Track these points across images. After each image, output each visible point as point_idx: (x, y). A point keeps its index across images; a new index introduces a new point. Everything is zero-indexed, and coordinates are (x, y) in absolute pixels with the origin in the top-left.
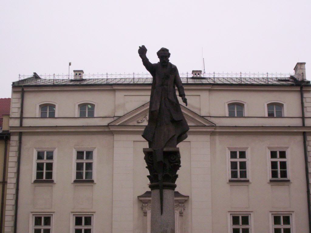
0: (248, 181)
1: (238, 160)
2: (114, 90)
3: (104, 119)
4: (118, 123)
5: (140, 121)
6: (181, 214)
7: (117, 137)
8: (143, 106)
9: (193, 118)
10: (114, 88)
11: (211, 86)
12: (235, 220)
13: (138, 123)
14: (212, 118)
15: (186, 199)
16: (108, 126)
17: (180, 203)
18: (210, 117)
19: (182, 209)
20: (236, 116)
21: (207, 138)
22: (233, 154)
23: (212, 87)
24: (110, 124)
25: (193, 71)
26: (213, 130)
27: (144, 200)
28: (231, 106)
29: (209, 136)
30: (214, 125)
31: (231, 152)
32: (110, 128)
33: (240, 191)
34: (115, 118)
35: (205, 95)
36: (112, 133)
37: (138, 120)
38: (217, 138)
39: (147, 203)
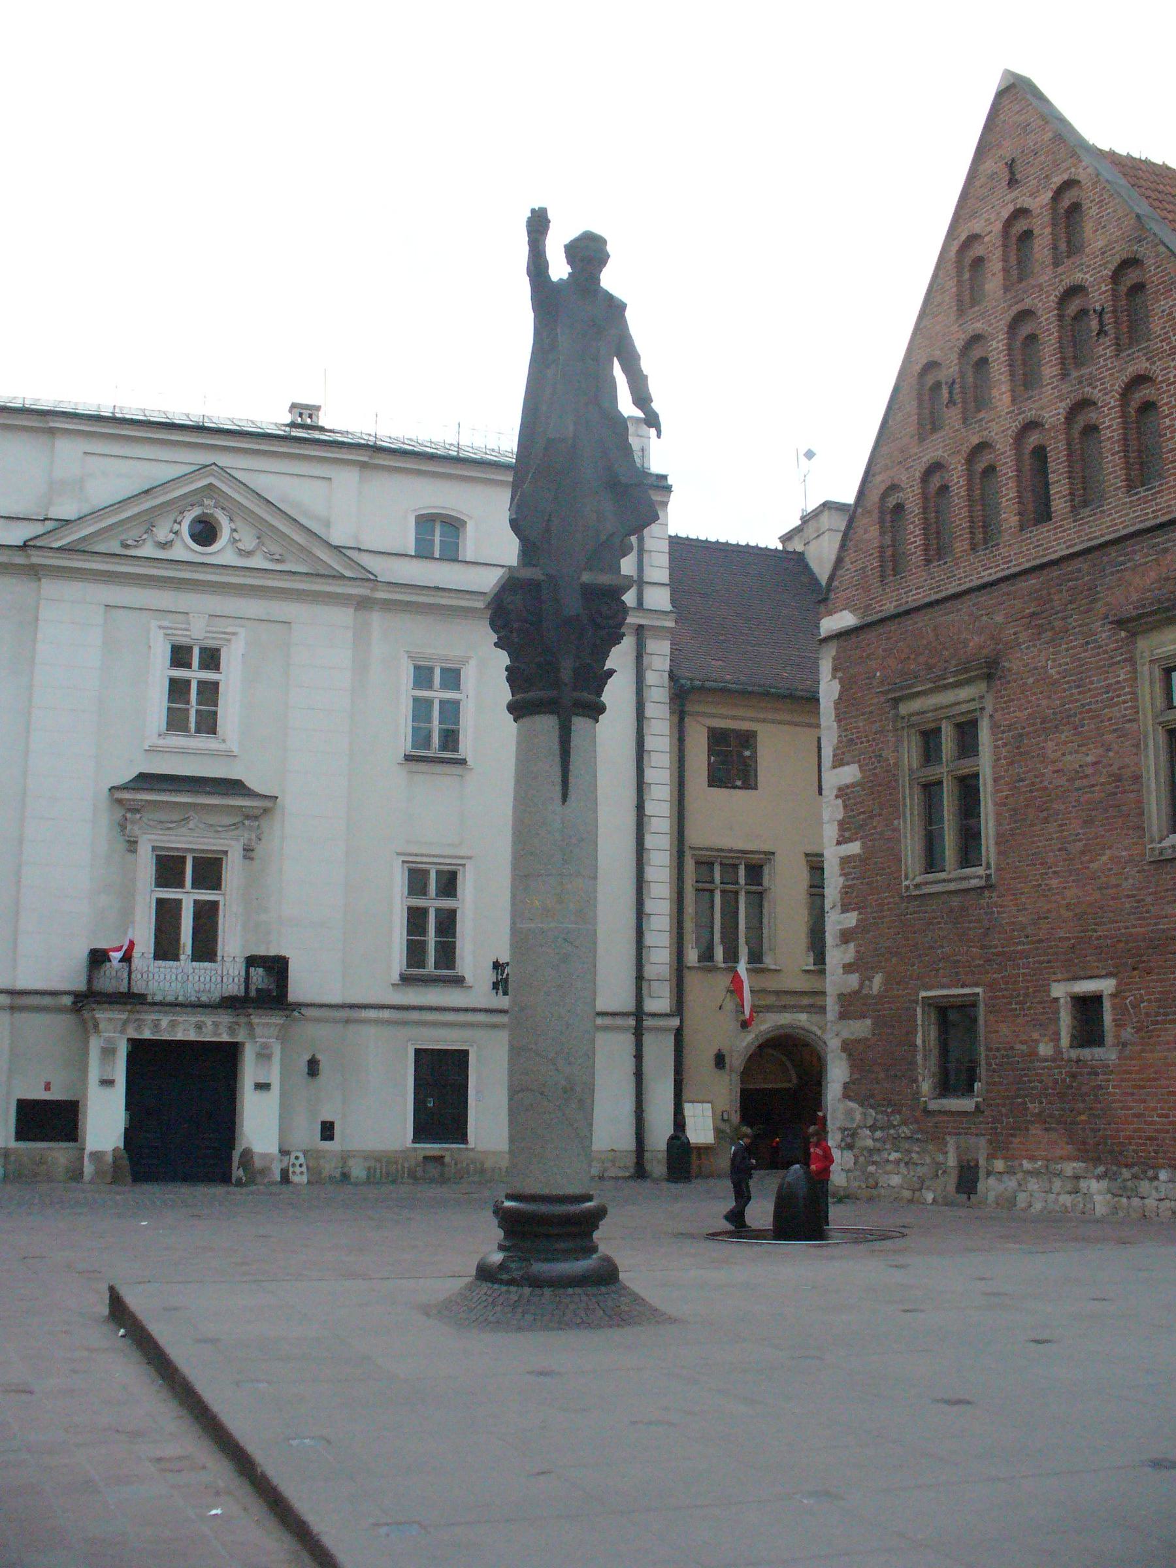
0: (463, 762)
1: (438, 695)
2: (52, 431)
3: (13, 524)
4: (57, 540)
5: (129, 542)
6: (248, 852)
7: (50, 587)
8: (147, 492)
9: (303, 549)
10: (52, 425)
11: (369, 453)
12: (417, 880)
13: (126, 546)
14: (364, 555)
15: (267, 804)
16: (25, 546)
17: (248, 817)
18: (359, 549)
19: (254, 837)
20: (437, 555)
21: (344, 616)
22: (423, 676)
23: (370, 457)
24: (30, 543)
25: (294, 406)
26: (367, 592)
27: (129, 800)
28: (425, 522)
29: (352, 610)
30: (372, 577)
31: (417, 668)
32: (29, 557)
33: (435, 792)
34: (50, 525)
35: (346, 479)
36: (34, 572)
37: (124, 537)
38: (376, 619)
39: (138, 811)
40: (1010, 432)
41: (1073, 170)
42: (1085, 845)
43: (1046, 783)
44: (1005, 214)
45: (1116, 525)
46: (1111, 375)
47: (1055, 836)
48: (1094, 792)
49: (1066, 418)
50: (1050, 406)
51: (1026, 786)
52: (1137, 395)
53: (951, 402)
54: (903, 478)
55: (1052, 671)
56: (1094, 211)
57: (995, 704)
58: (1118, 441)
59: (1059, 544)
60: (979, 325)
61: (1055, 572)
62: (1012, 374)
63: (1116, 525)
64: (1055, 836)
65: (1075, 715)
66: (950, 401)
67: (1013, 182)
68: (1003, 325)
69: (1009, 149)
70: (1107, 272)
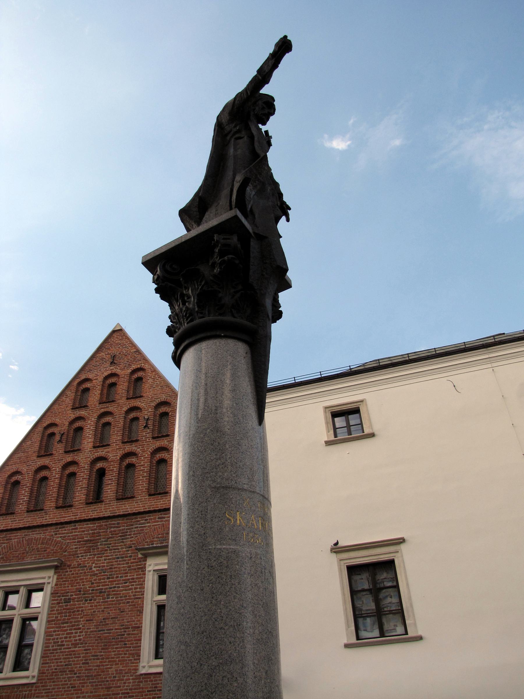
40: (89, 459)
41: (143, 365)
42: (101, 662)
43: (81, 626)
44: (106, 374)
45: (140, 507)
46: (147, 444)
47: (82, 655)
48: (110, 633)
49: (120, 458)
50: (114, 452)
51: (68, 627)
52: (158, 456)
53: (60, 441)
54: (24, 469)
55: (94, 569)
56: (150, 381)
57: (57, 582)
58: (147, 472)
59: (107, 511)
60: (83, 413)
61: (103, 523)
62: (95, 435)
63: (140, 507)
64: (82, 655)
65: (105, 592)
66: (60, 441)
67: (112, 363)
68: (96, 415)
69: (114, 351)
70: (153, 404)
